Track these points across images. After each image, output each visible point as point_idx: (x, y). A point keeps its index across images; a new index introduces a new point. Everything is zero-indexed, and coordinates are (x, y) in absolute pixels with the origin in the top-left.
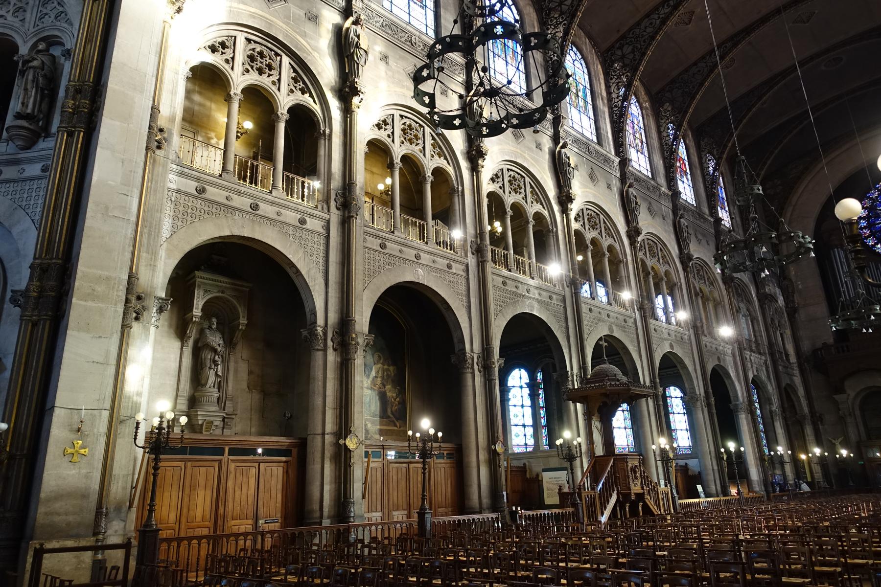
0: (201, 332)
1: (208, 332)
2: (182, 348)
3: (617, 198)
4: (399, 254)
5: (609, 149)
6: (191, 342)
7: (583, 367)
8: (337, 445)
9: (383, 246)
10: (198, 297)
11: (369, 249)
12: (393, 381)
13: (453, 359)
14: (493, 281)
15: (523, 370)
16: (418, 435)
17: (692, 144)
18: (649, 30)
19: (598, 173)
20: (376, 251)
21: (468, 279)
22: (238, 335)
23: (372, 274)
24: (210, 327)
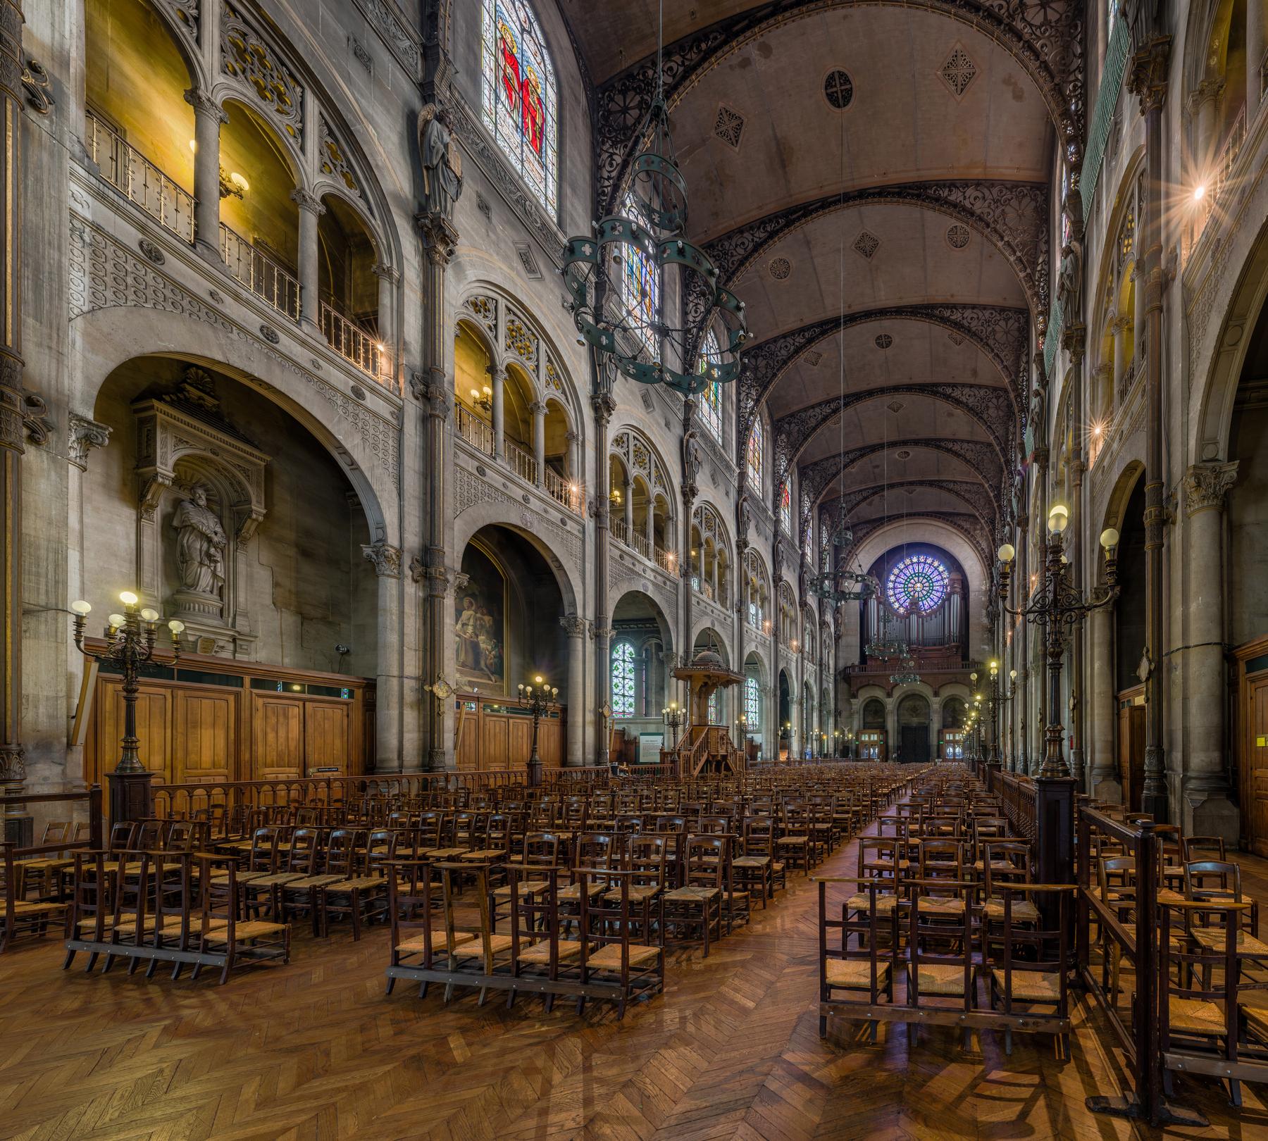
0: (177, 503)
1: (190, 507)
2: (138, 520)
3: (733, 507)
4: (502, 488)
5: (732, 457)
6: (157, 515)
7: (687, 651)
8: (420, 690)
9: (481, 471)
10: (164, 445)
11: (462, 469)
12: (488, 632)
13: (562, 622)
14: (610, 552)
15: (627, 646)
16: (529, 689)
17: (796, 481)
18: (783, 352)
19: (719, 479)
20: (471, 474)
21: (584, 542)
22: (250, 527)
23: (467, 502)
24: (193, 501)
